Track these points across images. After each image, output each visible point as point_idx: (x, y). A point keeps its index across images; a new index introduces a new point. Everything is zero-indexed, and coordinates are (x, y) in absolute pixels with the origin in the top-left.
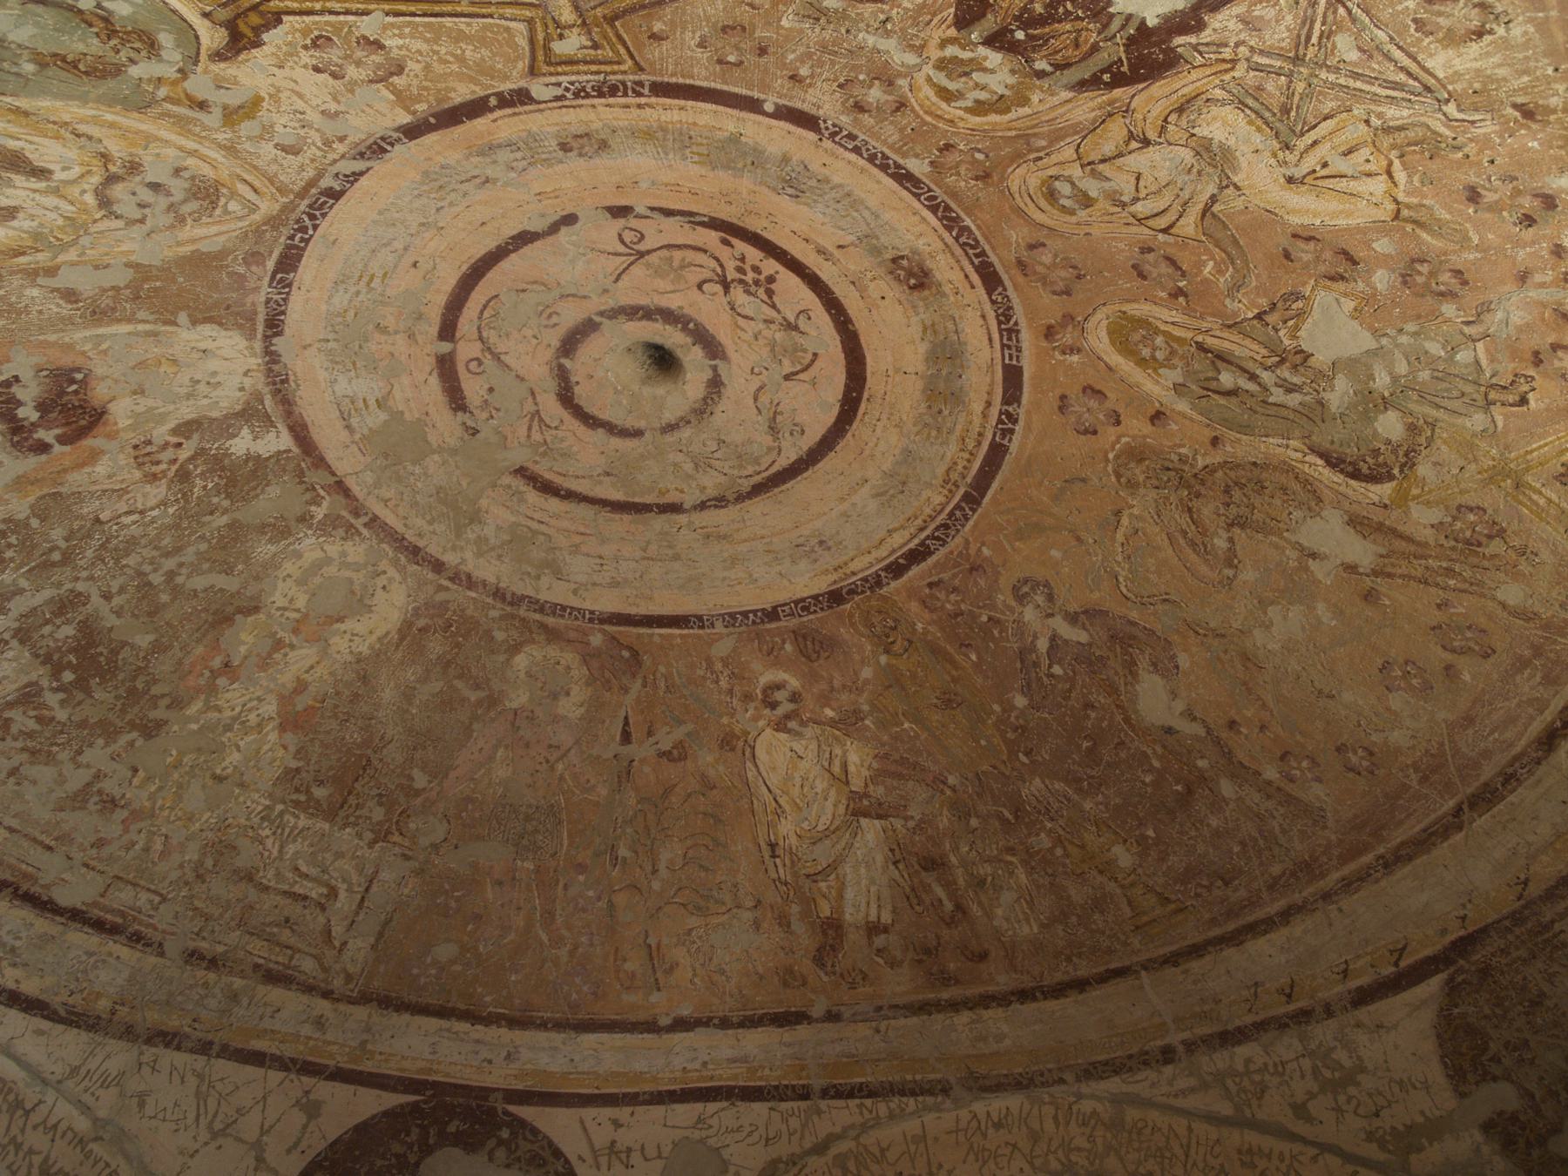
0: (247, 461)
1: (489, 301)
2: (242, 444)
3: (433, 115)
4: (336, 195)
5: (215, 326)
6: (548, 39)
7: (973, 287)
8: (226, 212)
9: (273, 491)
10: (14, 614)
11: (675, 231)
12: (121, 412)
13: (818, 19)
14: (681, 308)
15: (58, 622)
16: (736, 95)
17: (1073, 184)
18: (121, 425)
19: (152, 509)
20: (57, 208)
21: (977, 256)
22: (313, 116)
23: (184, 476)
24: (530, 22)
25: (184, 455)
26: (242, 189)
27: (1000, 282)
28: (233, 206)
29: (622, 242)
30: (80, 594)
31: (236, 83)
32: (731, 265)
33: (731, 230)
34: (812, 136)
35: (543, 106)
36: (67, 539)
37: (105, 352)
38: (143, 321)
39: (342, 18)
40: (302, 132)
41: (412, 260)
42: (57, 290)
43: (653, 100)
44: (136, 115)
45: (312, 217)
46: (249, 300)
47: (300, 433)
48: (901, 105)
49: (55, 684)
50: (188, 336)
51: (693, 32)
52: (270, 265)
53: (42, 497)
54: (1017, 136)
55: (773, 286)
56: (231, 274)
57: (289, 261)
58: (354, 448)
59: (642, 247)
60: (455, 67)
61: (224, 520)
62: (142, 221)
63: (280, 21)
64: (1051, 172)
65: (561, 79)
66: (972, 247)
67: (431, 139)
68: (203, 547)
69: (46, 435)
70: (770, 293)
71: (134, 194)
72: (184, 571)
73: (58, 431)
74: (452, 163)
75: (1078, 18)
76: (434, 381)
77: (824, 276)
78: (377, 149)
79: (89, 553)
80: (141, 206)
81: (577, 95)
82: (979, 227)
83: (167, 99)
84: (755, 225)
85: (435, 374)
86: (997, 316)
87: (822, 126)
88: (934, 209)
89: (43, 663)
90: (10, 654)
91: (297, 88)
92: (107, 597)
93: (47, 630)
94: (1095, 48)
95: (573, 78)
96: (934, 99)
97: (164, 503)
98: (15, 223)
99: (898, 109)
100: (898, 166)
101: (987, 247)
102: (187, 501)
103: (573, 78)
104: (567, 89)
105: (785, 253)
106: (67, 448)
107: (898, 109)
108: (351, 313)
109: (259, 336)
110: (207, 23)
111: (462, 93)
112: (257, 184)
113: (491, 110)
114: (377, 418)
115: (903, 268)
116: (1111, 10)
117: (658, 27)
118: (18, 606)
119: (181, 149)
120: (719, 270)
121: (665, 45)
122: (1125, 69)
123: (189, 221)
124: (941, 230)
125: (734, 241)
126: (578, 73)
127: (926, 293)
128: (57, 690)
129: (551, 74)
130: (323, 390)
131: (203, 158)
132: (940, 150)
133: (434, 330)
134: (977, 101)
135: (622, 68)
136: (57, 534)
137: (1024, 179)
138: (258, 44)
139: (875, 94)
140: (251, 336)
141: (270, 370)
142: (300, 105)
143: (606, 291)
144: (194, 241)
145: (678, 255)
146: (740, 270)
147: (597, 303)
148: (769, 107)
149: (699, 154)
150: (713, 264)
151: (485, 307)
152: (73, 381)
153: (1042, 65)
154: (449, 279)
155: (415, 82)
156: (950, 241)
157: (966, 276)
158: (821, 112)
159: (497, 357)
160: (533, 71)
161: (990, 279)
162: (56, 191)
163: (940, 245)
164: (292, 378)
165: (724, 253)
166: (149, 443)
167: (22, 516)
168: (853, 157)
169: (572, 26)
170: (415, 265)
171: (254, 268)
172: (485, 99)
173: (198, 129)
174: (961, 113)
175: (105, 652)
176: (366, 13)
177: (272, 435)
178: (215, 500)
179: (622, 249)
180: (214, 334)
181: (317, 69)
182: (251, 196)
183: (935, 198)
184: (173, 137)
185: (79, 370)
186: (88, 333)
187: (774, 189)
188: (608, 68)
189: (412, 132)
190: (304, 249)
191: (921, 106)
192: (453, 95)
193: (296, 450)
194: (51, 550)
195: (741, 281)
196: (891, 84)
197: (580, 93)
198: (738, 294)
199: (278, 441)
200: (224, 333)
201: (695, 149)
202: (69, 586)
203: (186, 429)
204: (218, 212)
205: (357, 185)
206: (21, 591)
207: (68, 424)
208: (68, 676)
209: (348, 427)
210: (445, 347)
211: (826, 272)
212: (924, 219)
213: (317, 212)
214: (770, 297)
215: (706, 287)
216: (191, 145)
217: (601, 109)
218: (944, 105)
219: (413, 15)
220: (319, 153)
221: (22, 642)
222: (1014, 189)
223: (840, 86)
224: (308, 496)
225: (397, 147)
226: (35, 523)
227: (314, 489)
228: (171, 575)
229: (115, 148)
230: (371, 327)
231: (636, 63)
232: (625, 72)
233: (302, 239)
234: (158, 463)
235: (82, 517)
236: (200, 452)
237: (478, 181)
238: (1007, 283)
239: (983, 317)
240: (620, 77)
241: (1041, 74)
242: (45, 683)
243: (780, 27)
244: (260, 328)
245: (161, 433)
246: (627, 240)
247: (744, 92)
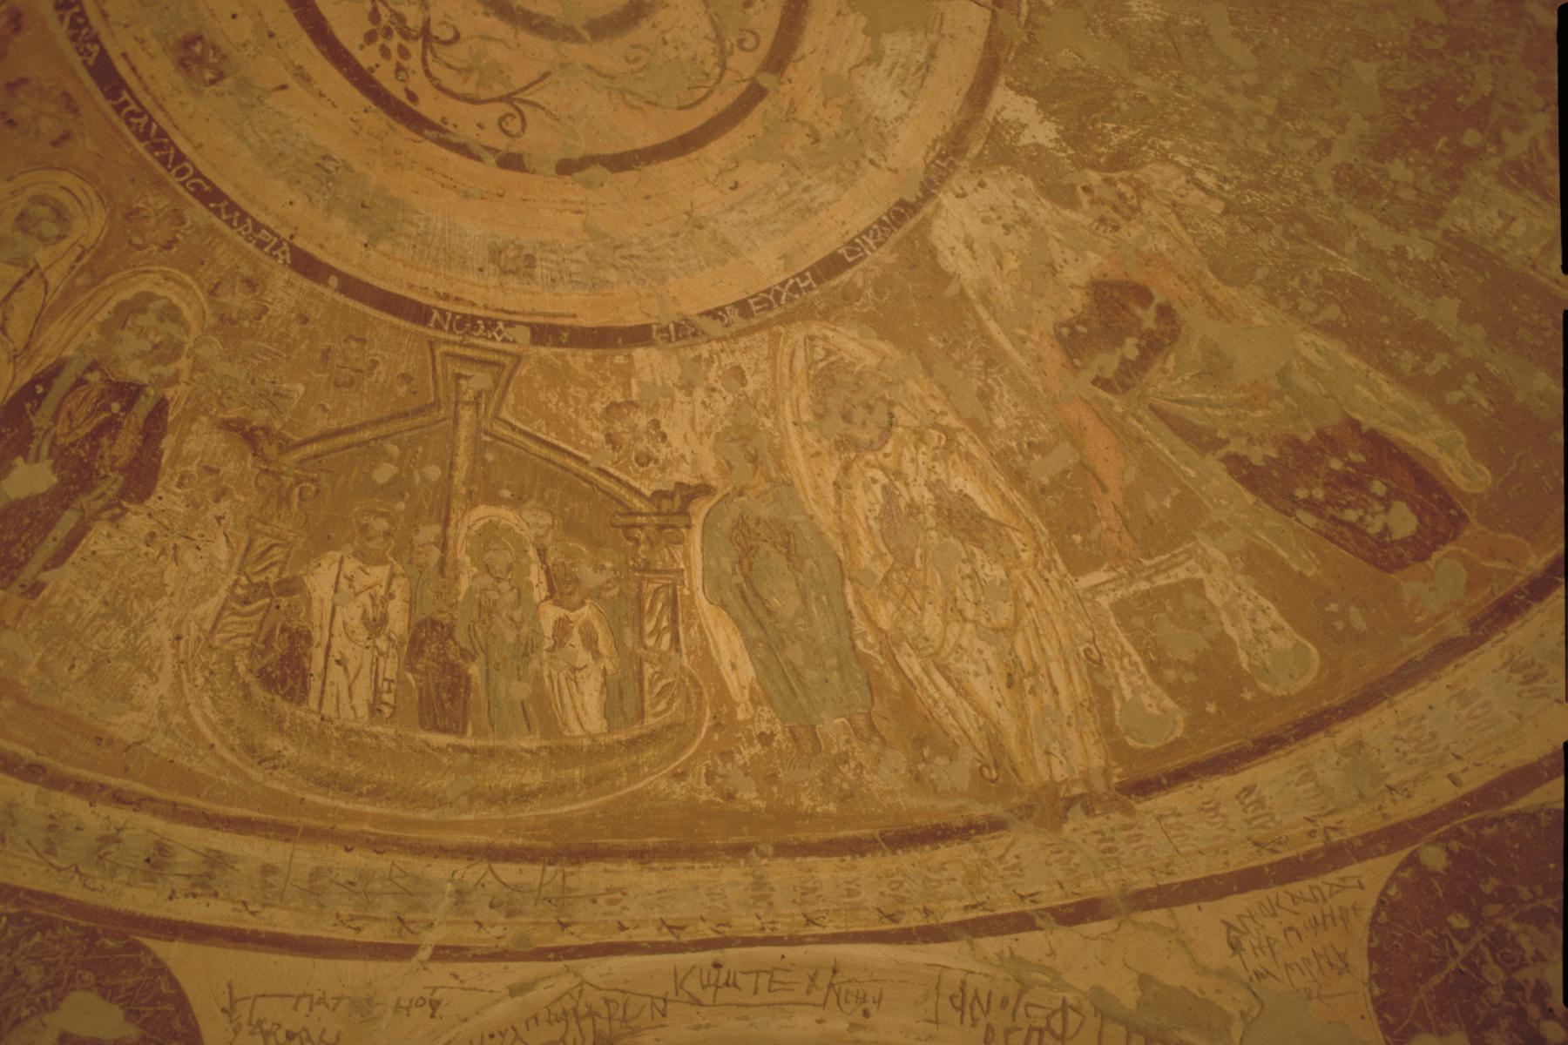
0: (1052, 113)
1: (692, 106)
2: (1041, 132)
3: (617, 346)
4: (743, 307)
5: (940, 260)
6: (490, 393)
7: (124, 55)
8: (829, 353)
9: (1065, 57)
10: (1400, 239)
11: (465, 121)
12: (1080, 269)
13: (276, 394)
14: (486, 14)
15: (1387, 187)
16: (360, 299)
17: (41, 238)
18: (1099, 259)
19: (1178, 164)
20: (913, 460)
21: (126, 104)
22: (700, 394)
23: (1120, 160)
24: (496, 417)
25: (1094, 177)
26: (799, 364)
27: (92, 71)
28: (820, 353)
29: (523, 119)
30: (1337, 179)
31: (719, 463)
32: (414, 63)
33: (406, 115)
34: (299, 242)
35: (526, 319)
36: (1269, 229)
37: (1029, 328)
38: (979, 320)
39: (617, 474)
40: (718, 386)
41: (735, 193)
42: (988, 409)
43: (433, 302)
44: (797, 483)
45: (778, 295)
46: (891, 259)
47: (979, 95)
48: (212, 293)
49: (1492, 150)
50: (965, 269)
51: (377, 381)
52: (845, 277)
53: (1226, 282)
54: (104, 278)
55: (370, 27)
56: (879, 293)
57: (832, 265)
58: (946, 30)
59: (505, 108)
60: (572, 390)
61: (1143, 83)
62: (883, 399)
63: (655, 493)
64: (65, 244)
65: (498, 345)
66: (132, 114)
67: (633, 319)
68: (1191, 81)
69: (1148, 318)
70: (374, 16)
71: (864, 423)
72: (1236, 82)
73: (1139, 311)
74: (633, 283)
75: (72, 445)
76: (806, 46)
77: (306, 42)
78: (684, 331)
79: (1274, 197)
80: (870, 408)
81: (495, 322)
82: (129, 144)
83: (769, 479)
84: (377, 120)
85: (798, 54)
86: (87, 23)
87: (288, 256)
88: (180, 157)
89: (1462, 176)
90: (1463, 222)
91: (689, 429)
92: (1326, 146)
93: (1406, 194)
94: (55, 417)
95: (489, 344)
96: (183, 306)
97: (1164, 158)
98: (943, 477)
99: (217, 286)
100: (217, 211)
101: (115, 118)
102: (1147, 134)
103: (489, 344)
104: (500, 333)
105: (348, 76)
106: (1154, 291)
107: (217, 286)
108: (828, 172)
109: (919, 216)
110: (694, 521)
111: (581, 360)
112: (786, 359)
113: (571, 328)
114: (897, 44)
115: (210, 66)
116: (51, 462)
117: (402, 390)
118: (1386, 240)
119: (801, 435)
120: (429, 57)
121: (402, 368)
122: (28, 406)
123: (858, 368)
124: (169, 129)
125: (403, 97)
126: (485, 349)
127: (179, 35)
128: (1499, 141)
129: (505, 353)
130: (912, 120)
131: (797, 412)
132: (175, 241)
133: (763, 105)
134: (144, 311)
135: (445, 348)
136: (1265, 243)
137: (90, 226)
138: (679, 485)
139: (237, 300)
140: (927, 222)
141: (942, 180)
142: (699, 410)
143: (563, 66)
144: (873, 350)
145: (469, 88)
146: (404, 52)
147: (579, 53)
148: (334, 281)
149: (412, 223)
150: (435, 68)
151: (699, 102)
152: (1074, 333)
153: (94, 377)
154: (716, 150)
155: (608, 389)
156: (159, 116)
157: (134, 69)
158: (288, 274)
159: (719, 38)
160: (518, 359)
161: (106, 75)
162: (898, 474)
163: (168, 107)
164: (932, 154)
165: (418, 82)
166: (1102, 220)
167: (1258, 290)
168: (262, 218)
169: (467, 403)
170: (735, 187)
171: (860, 284)
172: (571, 343)
173: (776, 441)
174: (160, 292)
175: (1409, 109)
176: (601, 471)
177: (1006, 115)
178: (1125, 107)
179: (526, 110)
180: (947, 253)
181: (664, 437)
182: (800, 354)
183: (182, 172)
184: (796, 445)
185: (1059, 336)
186: (1016, 355)
187: (347, 167)
188: (458, 350)
189: (639, 336)
190: (811, 269)
191: (194, 293)
192: (590, 360)
193: (1002, 80)
194: (1292, 238)
195: (406, 36)
196: (222, 318)
197: (491, 324)
198: (414, 18)
199: (1008, 104)
200: (940, 247)
201: (413, 230)
202: (1333, 198)
203: (1063, 196)
204: (833, 358)
205: (722, 304)
206: (1365, 247)
207: (1124, 307)
208: (1472, 137)
209: (932, 55)
210: (767, 80)
211: (304, 49)
212: (189, 140)
213: (769, 298)
214: (375, 10)
215: (449, 35)
216: (791, 428)
217: (480, 303)
218: (175, 300)
219: (570, 454)
220: (723, 356)
221: (1437, 213)
222: (98, 206)
223: (265, 310)
224: (1041, 19)
225: (664, 324)
226: (1261, 274)
227: (1028, 20)
228: (1252, 92)
229: (832, 473)
230: (823, 146)
231: (432, 351)
232: (447, 342)
233: (804, 278)
234: (1121, 196)
235: (1232, 232)
236: (1080, 164)
237: (625, 252)
238: (84, 75)
239: (105, 15)
240: (452, 337)
241: (92, 367)
242: (1494, 163)
243: (307, 385)
244: (911, 223)
245: (1081, 217)
246: (518, 121)
247: (352, 303)
